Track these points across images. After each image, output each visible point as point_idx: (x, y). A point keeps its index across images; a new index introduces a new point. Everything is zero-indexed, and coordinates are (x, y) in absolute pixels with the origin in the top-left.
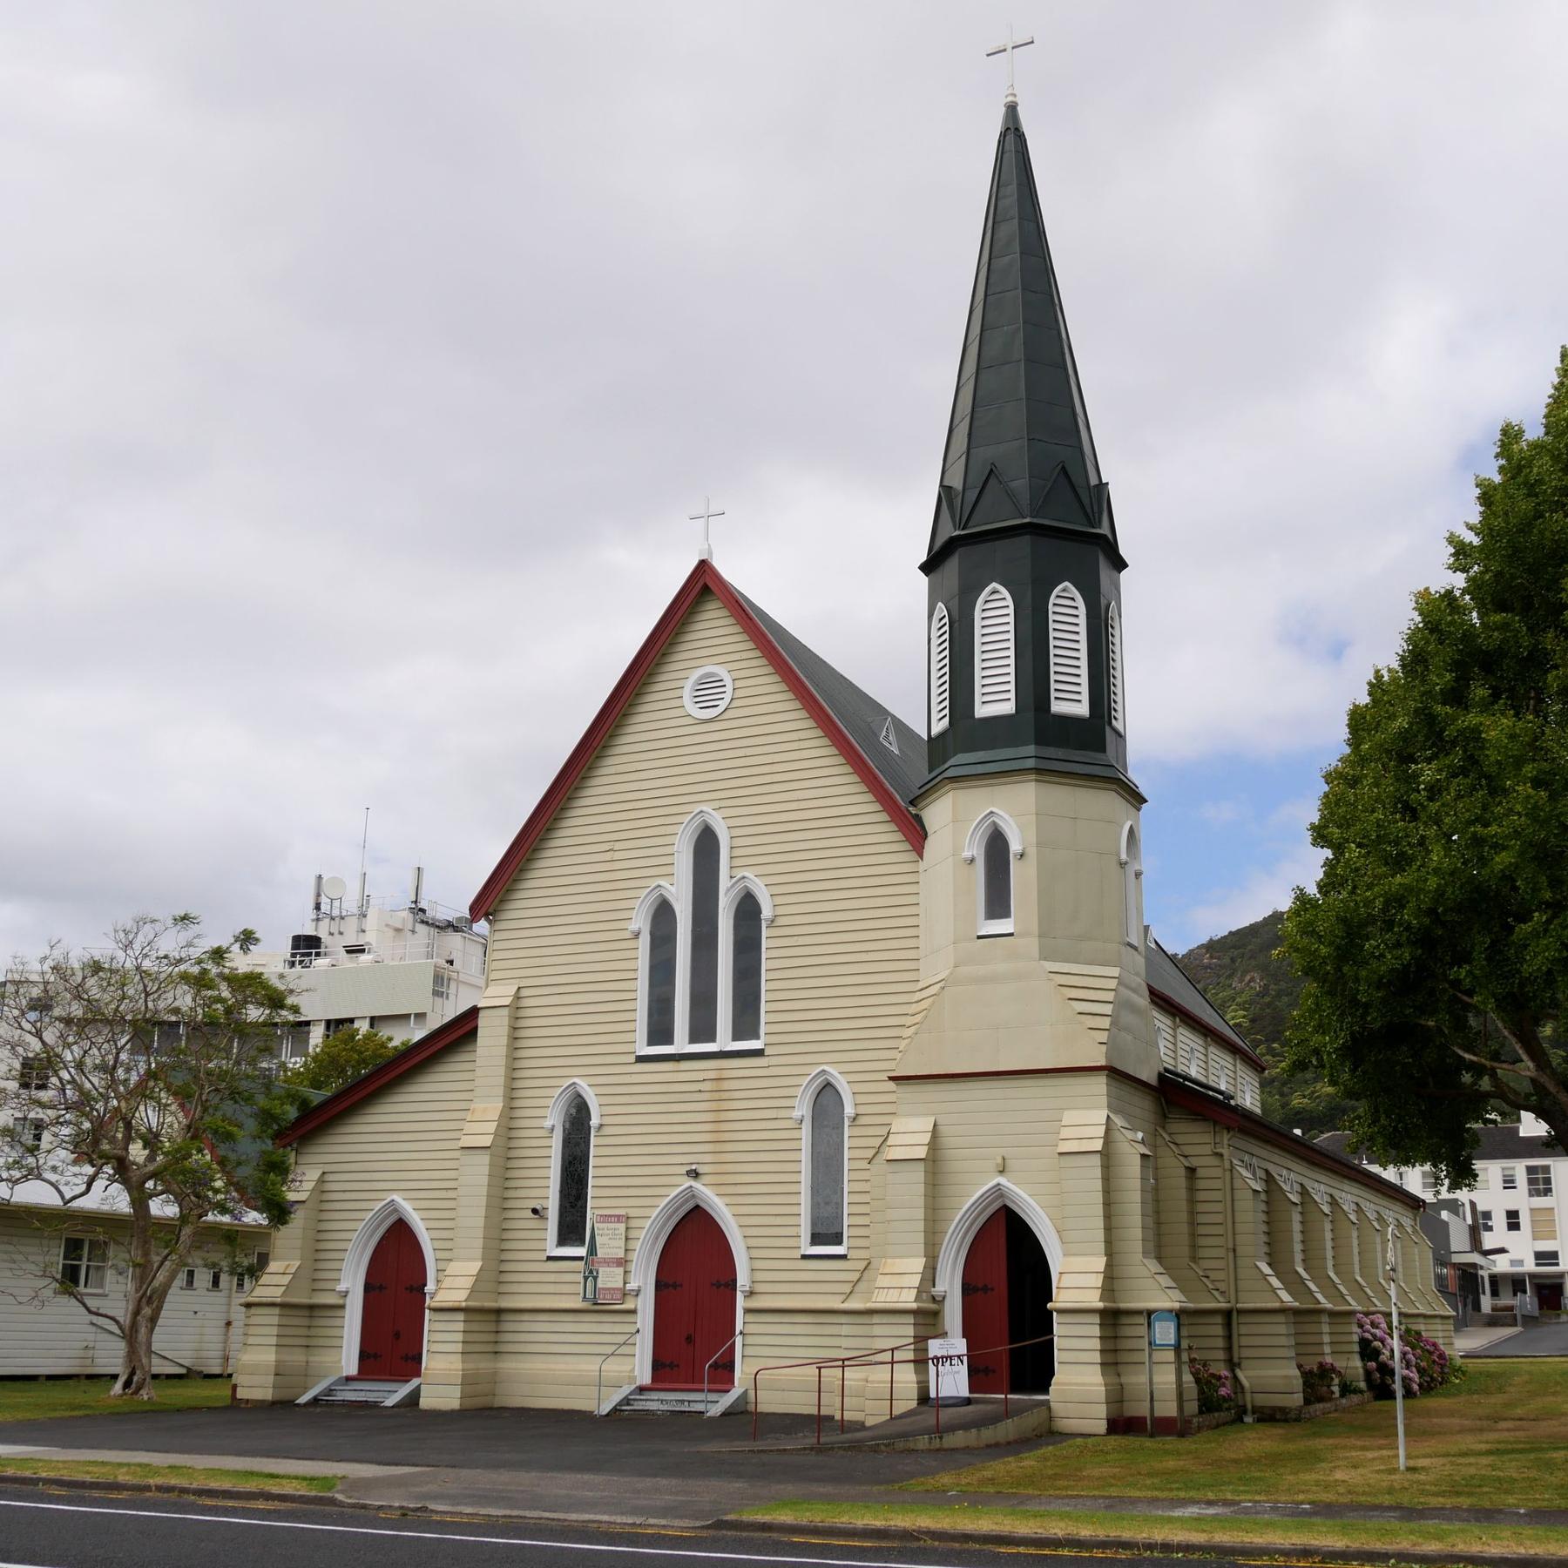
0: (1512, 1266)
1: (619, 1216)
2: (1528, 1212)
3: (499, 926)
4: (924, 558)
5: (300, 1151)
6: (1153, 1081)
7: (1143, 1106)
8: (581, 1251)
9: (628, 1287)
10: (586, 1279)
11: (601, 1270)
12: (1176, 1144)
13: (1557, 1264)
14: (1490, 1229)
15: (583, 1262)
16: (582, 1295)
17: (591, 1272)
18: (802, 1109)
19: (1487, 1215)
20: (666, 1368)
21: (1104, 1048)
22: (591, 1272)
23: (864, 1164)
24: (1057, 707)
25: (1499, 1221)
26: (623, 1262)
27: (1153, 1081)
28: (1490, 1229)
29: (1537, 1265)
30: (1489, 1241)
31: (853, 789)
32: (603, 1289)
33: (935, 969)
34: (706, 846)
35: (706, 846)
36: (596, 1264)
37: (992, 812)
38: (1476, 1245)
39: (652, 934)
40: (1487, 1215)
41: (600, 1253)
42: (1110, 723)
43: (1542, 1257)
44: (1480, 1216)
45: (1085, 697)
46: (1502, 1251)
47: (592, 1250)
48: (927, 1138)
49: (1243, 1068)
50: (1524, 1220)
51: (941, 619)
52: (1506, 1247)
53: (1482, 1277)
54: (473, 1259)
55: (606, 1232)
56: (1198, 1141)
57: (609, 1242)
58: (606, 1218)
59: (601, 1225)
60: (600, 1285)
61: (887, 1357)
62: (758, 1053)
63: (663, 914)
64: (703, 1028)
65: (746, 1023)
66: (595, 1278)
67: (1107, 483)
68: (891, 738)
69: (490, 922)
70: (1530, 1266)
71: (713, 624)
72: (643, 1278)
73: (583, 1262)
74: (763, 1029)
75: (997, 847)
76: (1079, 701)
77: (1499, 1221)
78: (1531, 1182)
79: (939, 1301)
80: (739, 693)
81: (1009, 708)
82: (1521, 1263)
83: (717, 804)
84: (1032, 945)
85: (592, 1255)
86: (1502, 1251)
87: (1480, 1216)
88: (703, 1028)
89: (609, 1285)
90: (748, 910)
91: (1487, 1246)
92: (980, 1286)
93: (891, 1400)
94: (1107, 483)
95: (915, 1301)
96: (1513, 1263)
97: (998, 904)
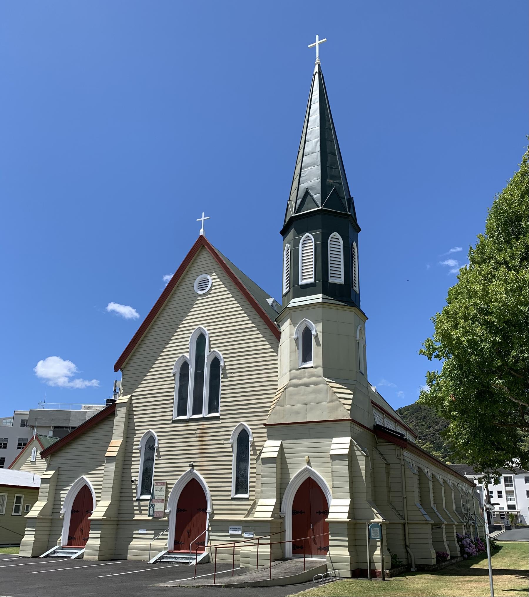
0: (500, 509)
1: (163, 483)
2: (497, 493)
3: (126, 373)
4: (282, 227)
5: (51, 459)
6: (372, 428)
7: (369, 436)
8: (148, 497)
9: (166, 511)
10: (150, 508)
11: (156, 504)
12: (381, 454)
13: (515, 509)
14: (492, 497)
15: (149, 502)
16: (148, 514)
17: (152, 505)
18: (233, 439)
19: (492, 492)
20: (178, 545)
21: (349, 412)
22: (152, 505)
23: (255, 462)
24: (330, 280)
25: (495, 494)
26: (165, 501)
27: (372, 428)
28: (492, 497)
29: (508, 509)
30: (493, 501)
31: (215, 267)
32: (156, 512)
33: (283, 381)
34: (201, 340)
35: (201, 340)
36: (154, 502)
37: (305, 320)
38: (489, 501)
39: (180, 374)
40: (492, 492)
41: (156, 497)
42: (353, 287)
43: (509, 506)
44: (490, 492)
45: (342, 276)
46: (498, 504)
47: (153, 497)
48: (277, 449)
49: (409, 436)
50: (504, 494)
51: (287, 251)
52: (499, 503)
53: (491, 513)
54: (109, 500)
55: (158, 489)
56: (390, 450)
57: (159, 494)
58: (158, 484)
59: (156, 487)
60: (155, 510)
61: (256, 541)
62: (217, 418)
63: (185, 366)
64: (197, 409)
65: (213, 408)
66: (153, 508)
67: (353, 198)
68: (275, 306)
69: (122, 372)
70: (506, 509)
71: (205, 258)
72: (171, 509)
73: (149, 502)
74: (220, 409)
75: (307, 335)
76: (340, 278)
77: (495, 494)
78: (505, 482)
79: (282, 518)
80: (214, 284)
81: (312, 280)
82: (503, 509)
83: (205, 325)
84: (320, 371)
85: (152, 498)
86: (498, 504)
87: (490, 492)
88: (197, 409)
89: (159, 510)
90: (216, 363)
91: (492, 502)
92: (322, 514)
93: (258, 559)
94: (353, 198)
95: (271, 517)
96: (500, 509)
97: (307, 356)
